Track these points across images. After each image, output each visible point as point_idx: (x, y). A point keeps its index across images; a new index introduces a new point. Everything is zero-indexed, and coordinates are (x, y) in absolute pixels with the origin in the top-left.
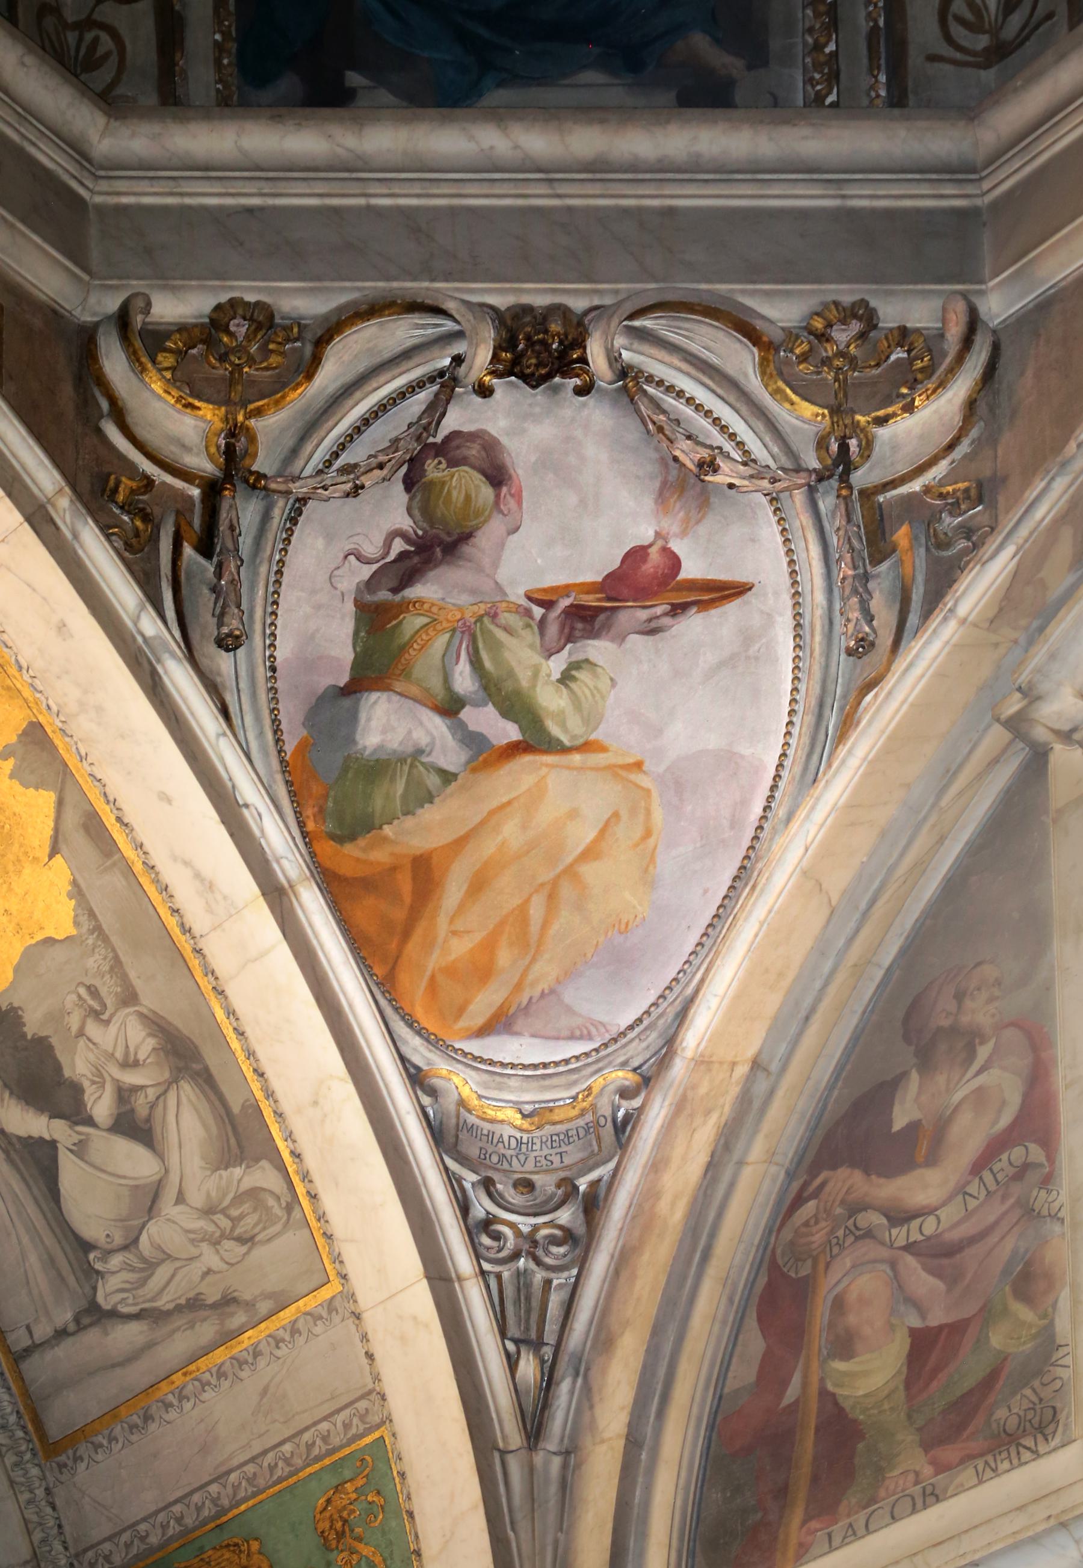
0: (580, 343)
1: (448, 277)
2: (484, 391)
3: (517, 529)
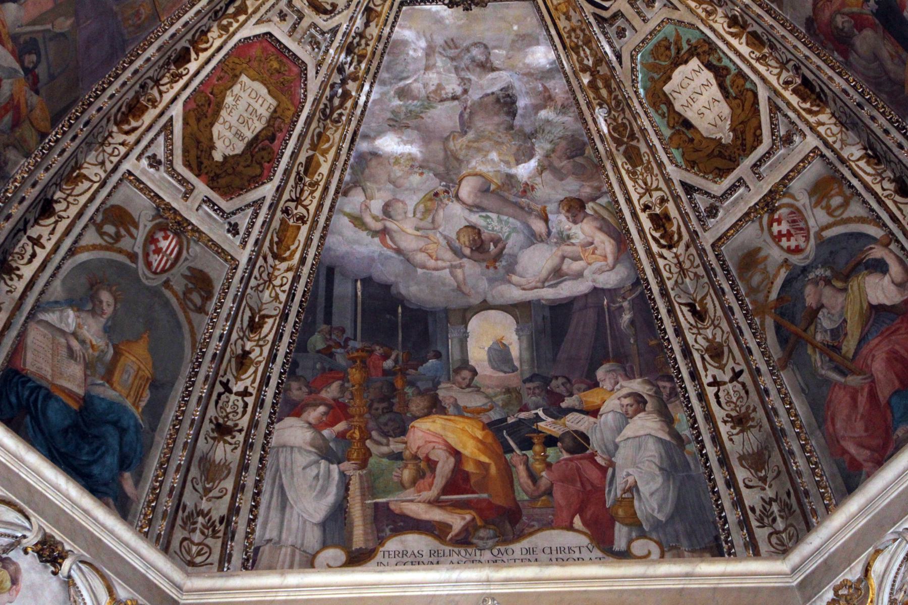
0: (64, 558)
1: (34, 511)
2: (26, 552)
3: (11, 602)
